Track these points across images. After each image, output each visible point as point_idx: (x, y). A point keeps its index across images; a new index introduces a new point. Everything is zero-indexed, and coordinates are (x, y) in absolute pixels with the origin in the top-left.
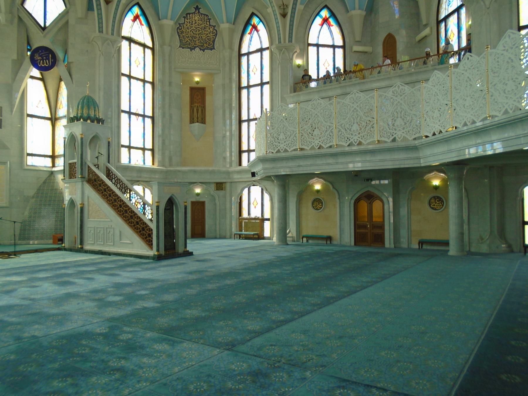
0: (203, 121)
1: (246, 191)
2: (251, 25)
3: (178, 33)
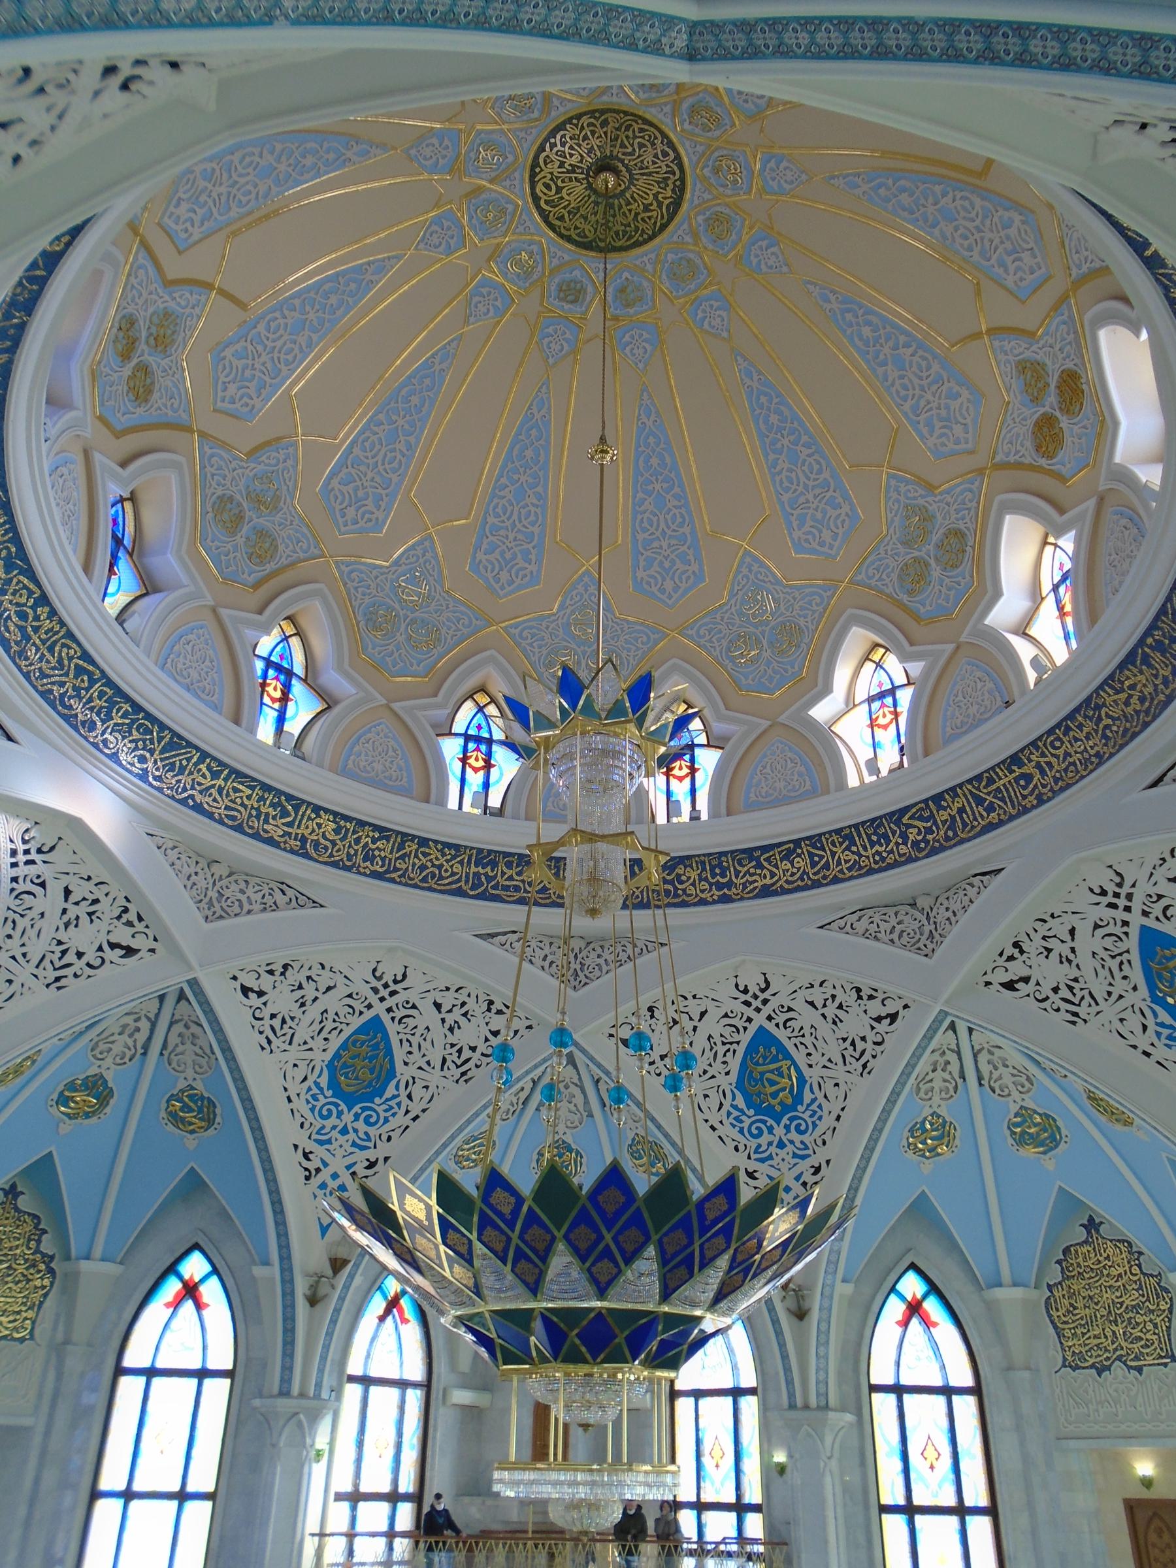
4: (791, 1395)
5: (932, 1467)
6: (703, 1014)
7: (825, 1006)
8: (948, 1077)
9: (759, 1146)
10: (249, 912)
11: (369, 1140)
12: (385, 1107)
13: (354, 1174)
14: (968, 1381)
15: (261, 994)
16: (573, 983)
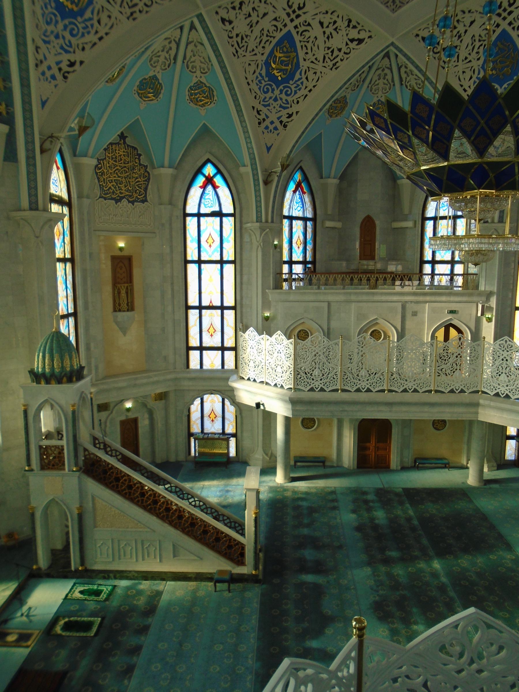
0: (131, 308)
1: (198, 401)
2: (204, 175)
3: (97, 173)
11: (288, 103)
12: (295, 85)
13: (281, 122)
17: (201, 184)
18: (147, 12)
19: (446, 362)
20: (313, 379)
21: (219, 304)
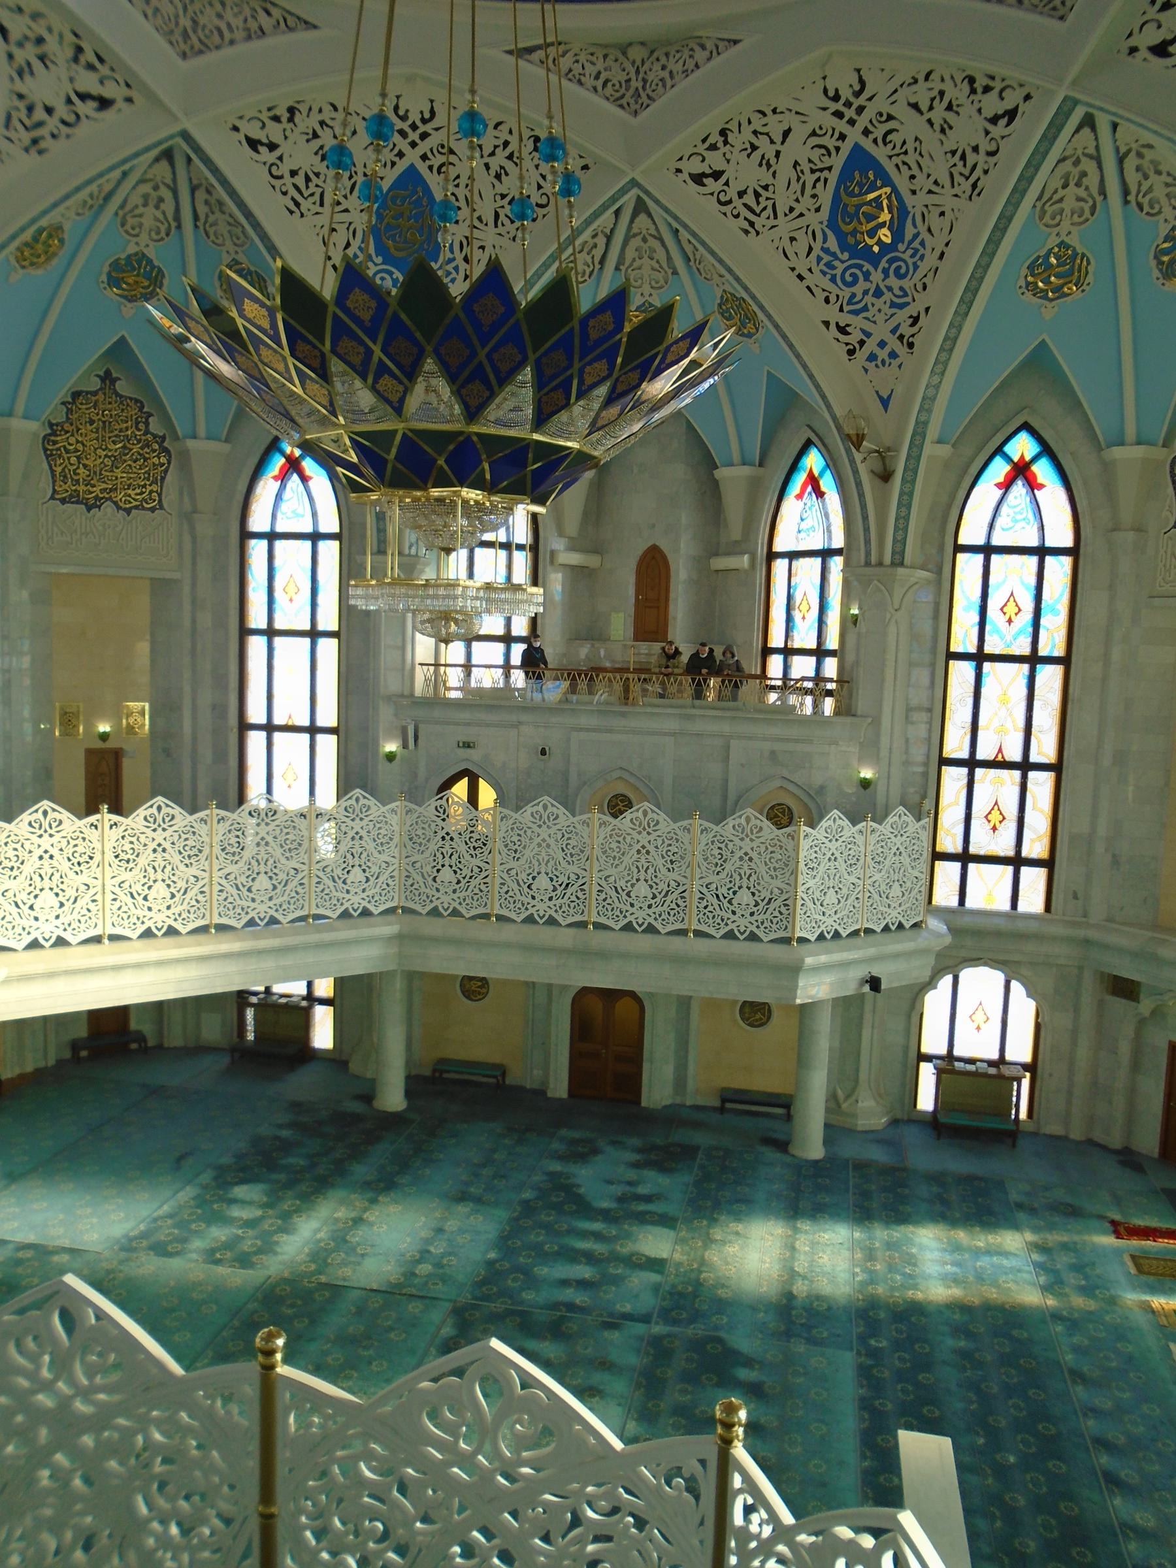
3: (45, 450)
4: (868, 553)
5: (1010, 621)
6: (786, 134)
7: (931, 108)
8: (1081, 192)
9: (854, 295)
10: (232, 42)
14: (1068, 541)
15: (272, 147)
16: (634, 107)
17: (276, 472)
18: (68, 136)
19: (616, 862)
20: (533, 898)
21: (306, 723)
